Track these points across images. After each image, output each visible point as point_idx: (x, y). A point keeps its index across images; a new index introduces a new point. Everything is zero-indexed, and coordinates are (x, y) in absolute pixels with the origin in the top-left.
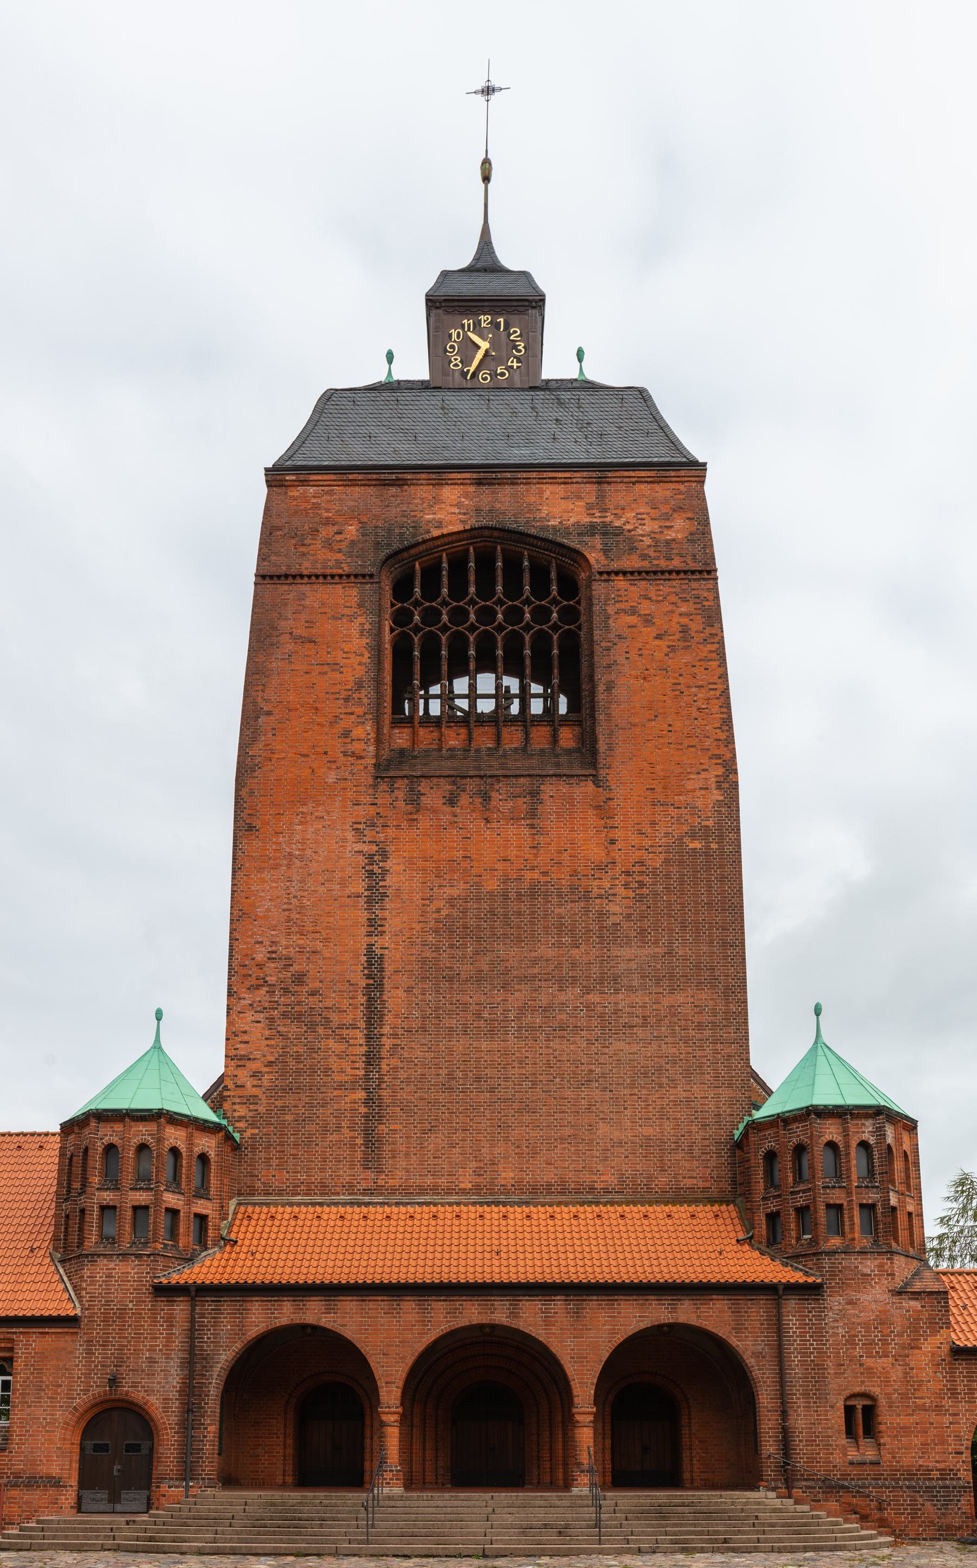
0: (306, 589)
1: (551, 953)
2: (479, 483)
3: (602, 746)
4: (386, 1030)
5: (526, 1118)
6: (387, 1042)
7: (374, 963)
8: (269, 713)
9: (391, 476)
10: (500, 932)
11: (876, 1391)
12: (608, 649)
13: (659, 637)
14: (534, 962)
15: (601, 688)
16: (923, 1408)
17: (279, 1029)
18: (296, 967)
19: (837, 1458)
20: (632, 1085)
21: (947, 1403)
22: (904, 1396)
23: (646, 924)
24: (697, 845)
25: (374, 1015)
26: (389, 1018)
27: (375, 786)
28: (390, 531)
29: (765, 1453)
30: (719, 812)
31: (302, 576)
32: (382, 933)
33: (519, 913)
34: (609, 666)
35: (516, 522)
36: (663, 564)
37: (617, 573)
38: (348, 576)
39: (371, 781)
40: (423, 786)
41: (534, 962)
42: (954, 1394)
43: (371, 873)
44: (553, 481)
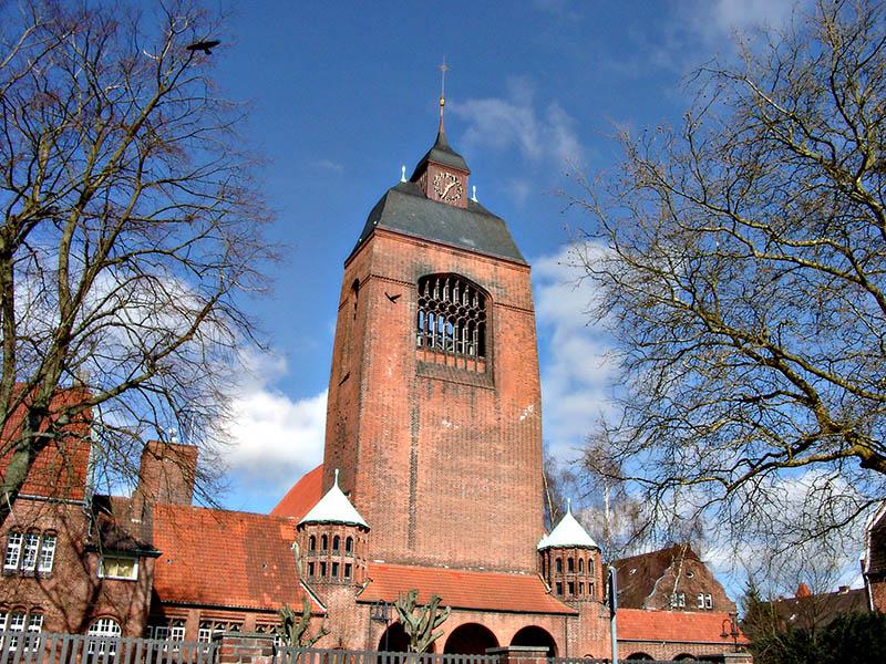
2: (454, 254)
14: (472, 466)
25: (413, 482)
26: (418, 484)
40: (433, 382)
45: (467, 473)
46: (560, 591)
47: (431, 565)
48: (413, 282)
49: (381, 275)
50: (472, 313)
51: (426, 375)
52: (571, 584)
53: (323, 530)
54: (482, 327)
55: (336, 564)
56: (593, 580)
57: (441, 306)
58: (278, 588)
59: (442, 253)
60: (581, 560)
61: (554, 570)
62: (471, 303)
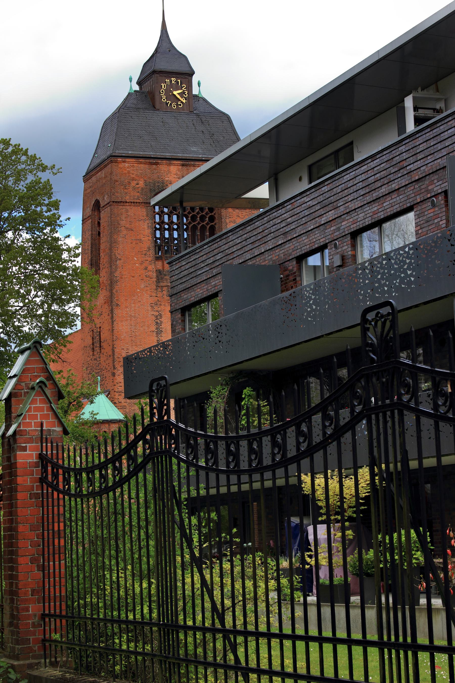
0: (128, 208)
2: (183, 165)
8: (120, 259)
9: (153, 160)
28: (154, 184)
39: (155, 287)
43: (157, 323)
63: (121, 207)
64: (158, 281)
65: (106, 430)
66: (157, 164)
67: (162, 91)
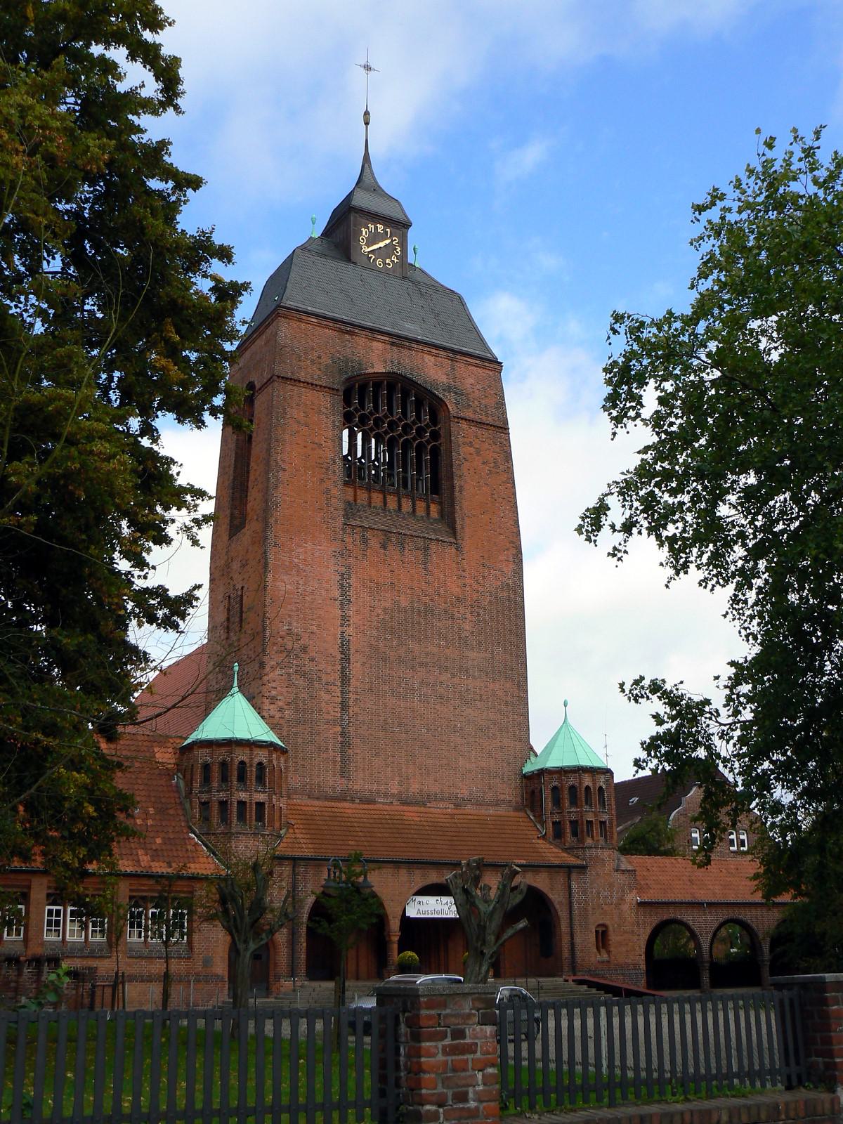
1: (436, 650)
2: (392, 344)
3: (458, 526)
4: (351, 689)
5: (424, 751)
6: (353, 696)
7: (345, 645)
8: (284, 470)
9: (348, 328)
10: (410, 633)
11: (608, 923)
12: (460, 465)
13: (484, 463)
14: (427, 655)
15: (457, 489)
16: (625, 932)
17: (294, 681)
18: (301, 642)
19: (593, 959)
20: (475, 736)
21: (636, 929)
22: (619, 926)
23: (481, 638)
24: (505, 594)
27: (343, 529)
28: (347, 363)
29: (564, 957)
30: (514, 577)
31: (300, 381)
32: (349, 625)
33: (419, 623)
34: (460, 476)
35: (412, 374)
36: (484, 419)
37: (462, 419)
38: (325, 387)
40: (369, 534)
41: (427, 655)
42: (638, 926)
43: (342, 585)
44: (429, 353)
45: (421, 664)
46: (558, 833)
47: (372, 802)
48: (336, 387)
49: (289, 375)
50: (420, 431)
51: (358, 523)
52: (574, 824)
53: (221, 754)
54: (435, 452)
55: (242, 804)
56: (605, 818)
57: (405, 427)
58: (159, 841)
59: (375, 344)
60: (588, 788)
61: (548, 804)
62: (418, 417)
63: (290, 387)
64: (346, 516)
65: (244, 758)
66: (351, 333)
67: (363, 239)
